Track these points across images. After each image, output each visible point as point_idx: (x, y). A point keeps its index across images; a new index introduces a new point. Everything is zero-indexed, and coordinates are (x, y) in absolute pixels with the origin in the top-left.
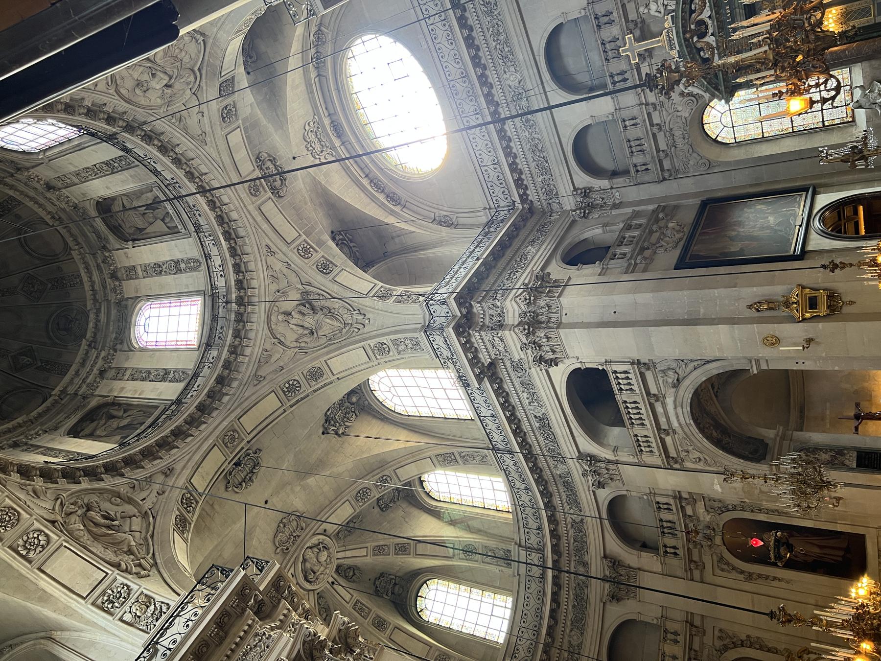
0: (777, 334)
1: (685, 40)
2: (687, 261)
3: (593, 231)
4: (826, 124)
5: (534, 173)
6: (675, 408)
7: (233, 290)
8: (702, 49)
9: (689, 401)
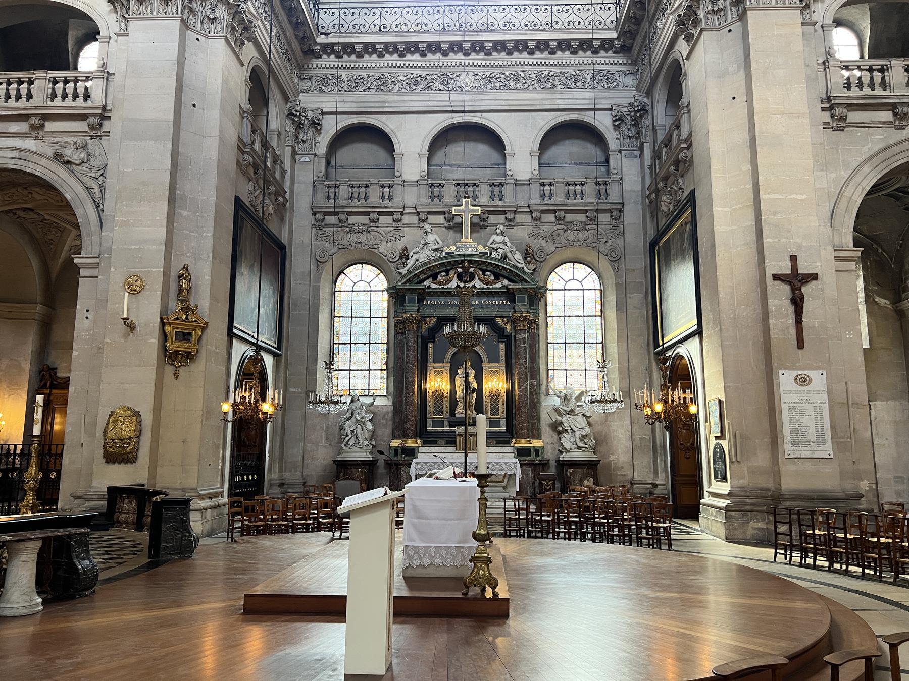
0: (145, 293)
1: (463, 261)
2: (241, 213)
3: (275, 118)
5: (354, 71)
6: (16, 149)
8: (448, 274)
9: (28, 170)
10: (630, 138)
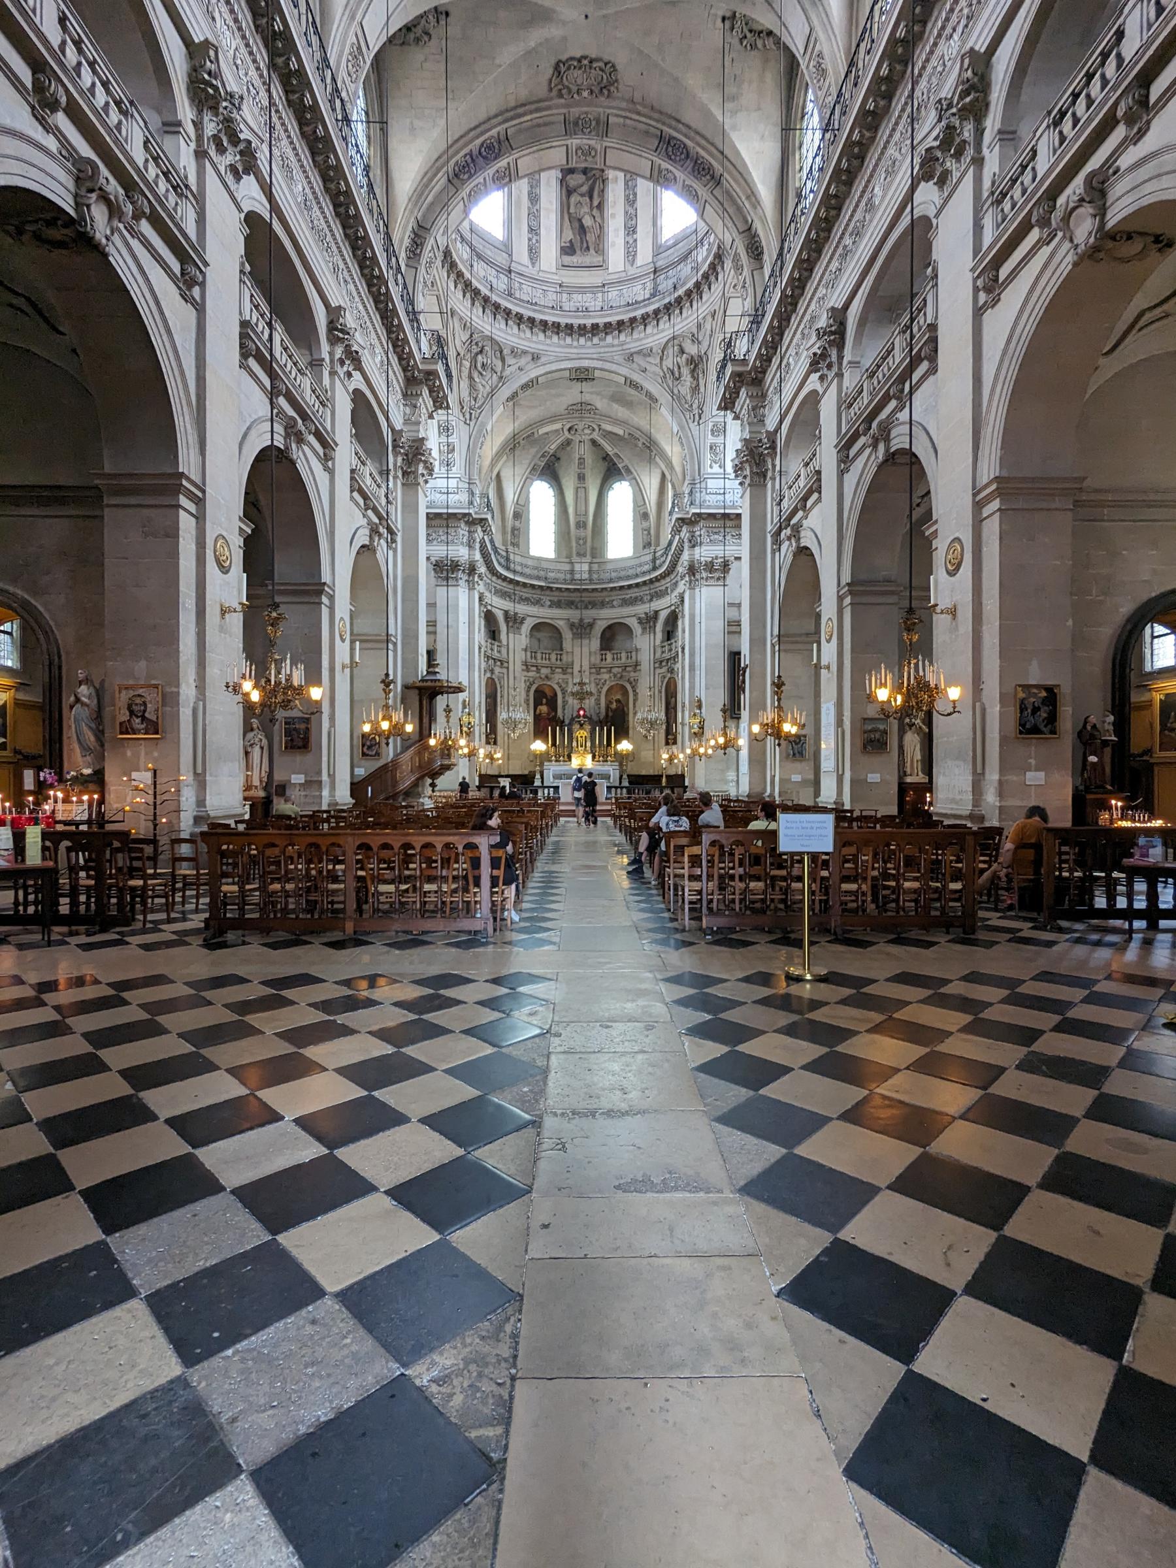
7: (685, 289)
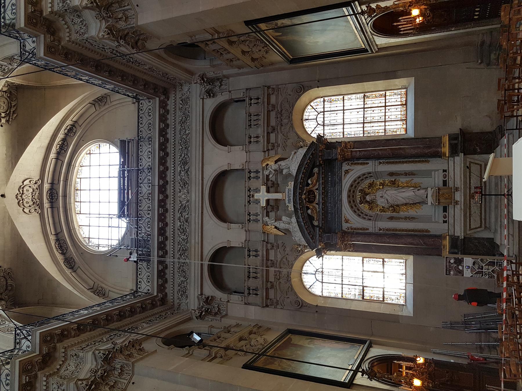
4: (381, 260)
10: (221, 85)
